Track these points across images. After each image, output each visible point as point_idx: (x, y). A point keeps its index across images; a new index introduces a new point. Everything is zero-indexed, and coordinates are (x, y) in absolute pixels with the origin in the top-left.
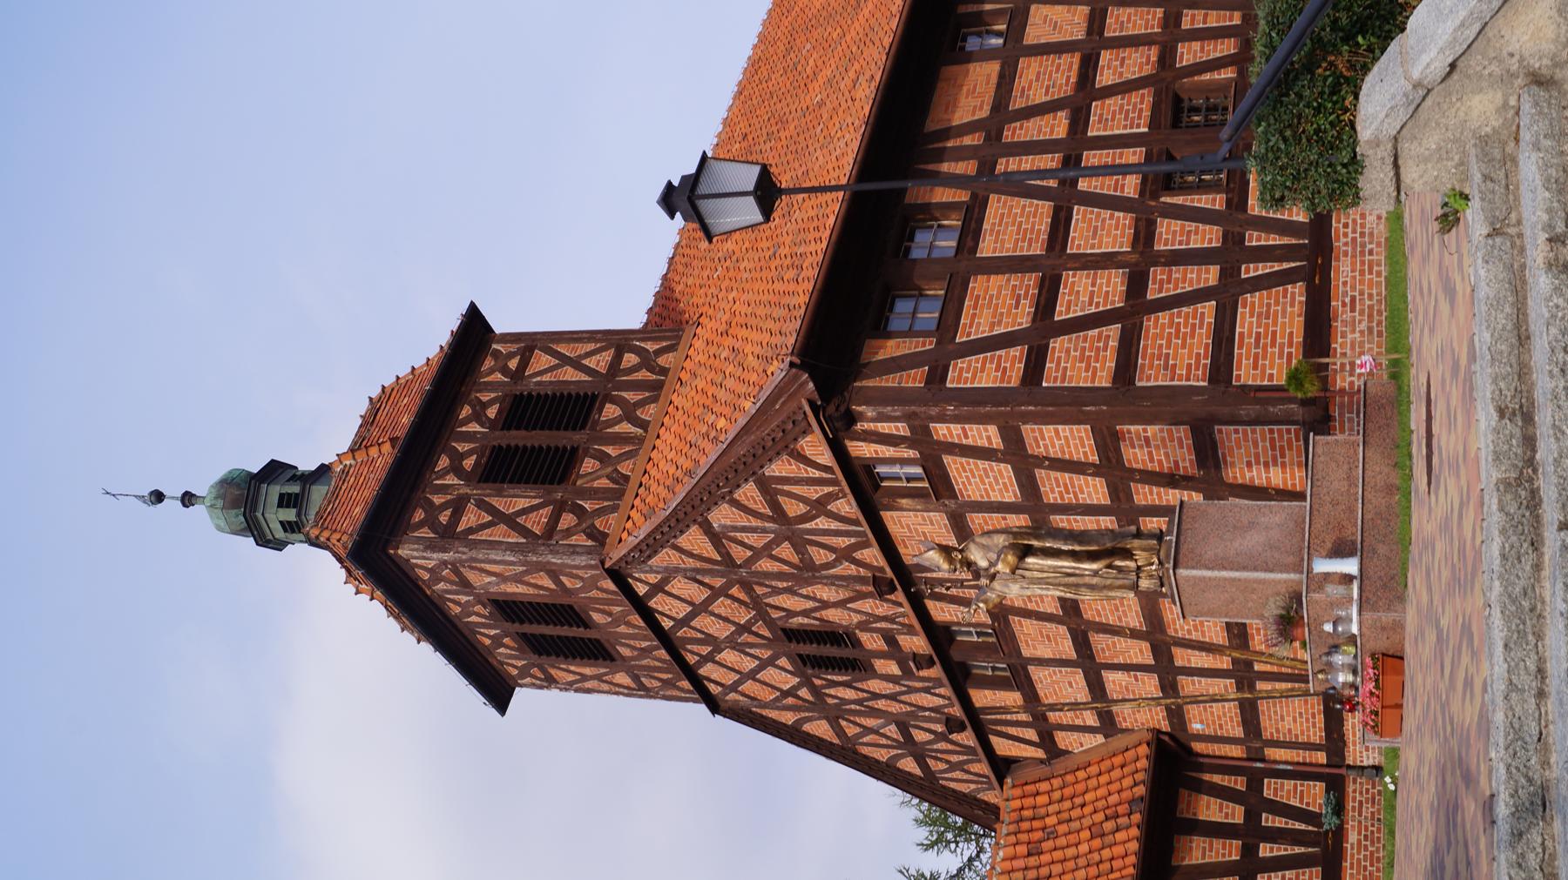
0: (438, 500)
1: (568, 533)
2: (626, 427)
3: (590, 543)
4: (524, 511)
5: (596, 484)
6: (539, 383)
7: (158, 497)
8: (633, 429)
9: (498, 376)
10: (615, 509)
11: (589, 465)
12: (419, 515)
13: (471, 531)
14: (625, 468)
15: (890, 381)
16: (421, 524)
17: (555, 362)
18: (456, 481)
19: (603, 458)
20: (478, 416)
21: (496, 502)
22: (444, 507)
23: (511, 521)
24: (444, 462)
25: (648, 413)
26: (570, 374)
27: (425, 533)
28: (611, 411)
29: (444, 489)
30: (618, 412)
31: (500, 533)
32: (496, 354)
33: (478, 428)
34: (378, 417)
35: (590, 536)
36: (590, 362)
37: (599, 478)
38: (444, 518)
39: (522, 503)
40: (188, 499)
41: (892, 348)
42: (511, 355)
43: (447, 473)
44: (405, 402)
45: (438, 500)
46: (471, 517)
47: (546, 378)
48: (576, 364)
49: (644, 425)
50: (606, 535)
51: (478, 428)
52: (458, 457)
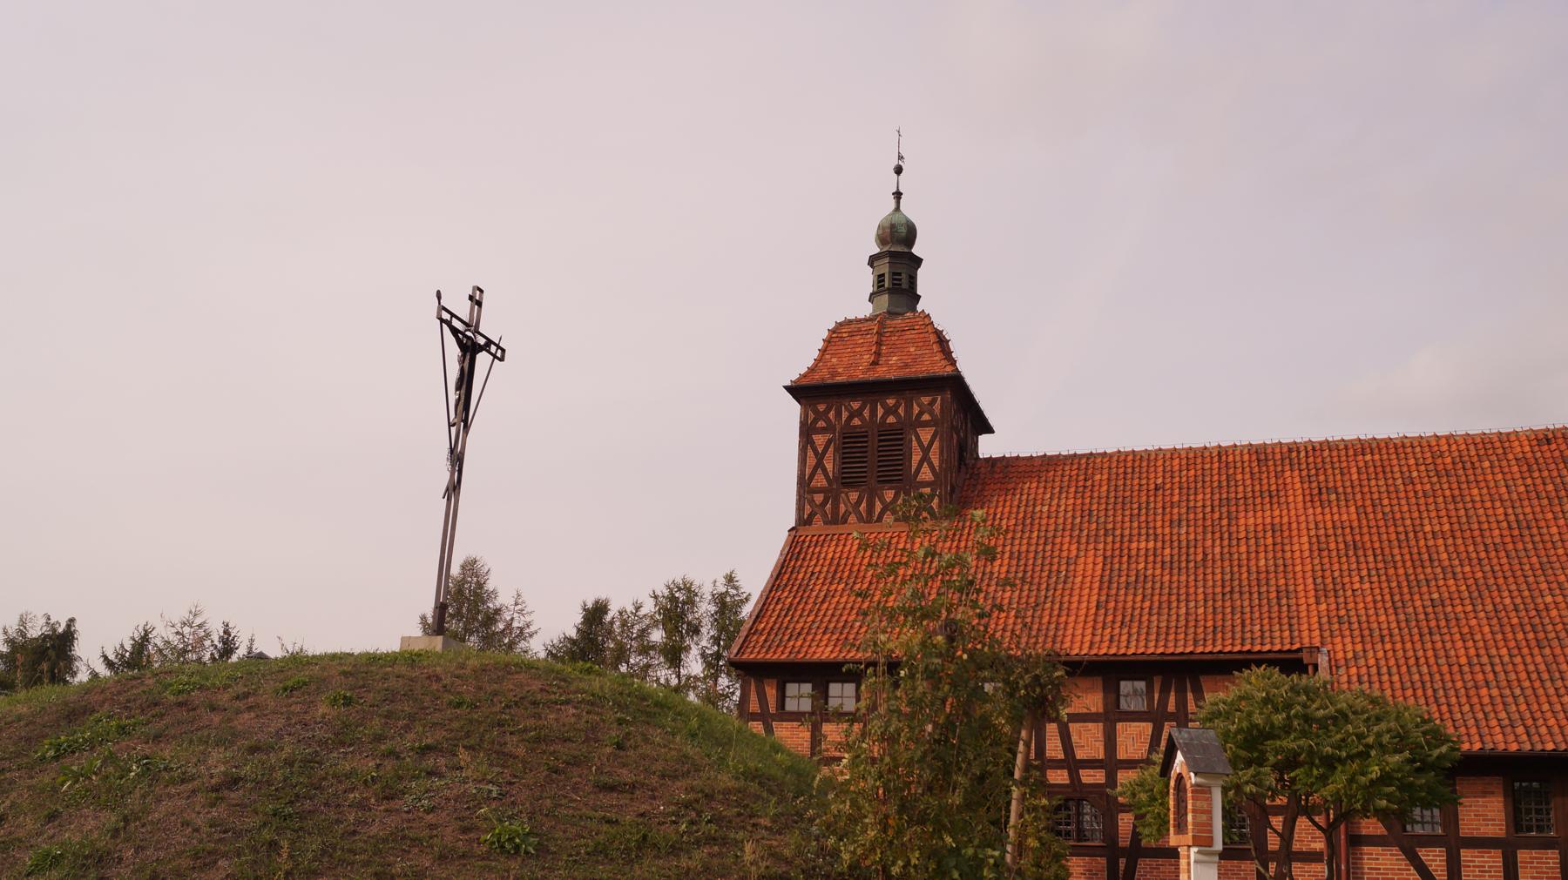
0: (832, 415)
1: (812, 502)
2: (878, 506)
3: (806, 517)
4: (825, 471)
5: (842, 505)
6: (911, 441)
7: (899, 170)
8: (877, 513)
9: (916, 410)
10: (825, 523)
11: (854, 496)
12: (821, 408)
13: (812, 443)
14: (852, 518)
15: (753, 697)
16: (816, 412)
17: (926, 444)
18: (844, 419)
19: (859, 503)
20: (889, 411)
21: (831, 449)
22: (828, 421)
23: (819, 464)
24: (856, 405)
25: (888, 519)
26: (916, 458)
27: (811, 416)
28: (889, 495)
29: (839, 414)
30: (888, 500)
31: (811, 460)
32: (932, 403)
33: (879, 416)
34: (908, 333)
35: (809, 515)
36: (925, 468)
37: (846, 505)
38: (821, 424)
39: (829, 467)
40: (898, 195)
41: (771, 693)
42: (931, 413)
43: (849, 411)
44: (912, 349)
45: (832, 415)
46: (820, 440)
47: (915, 443)
48: (925, 458)
49: (880, 519)
50: (810, 524)
51: (879, 416)
52: (859, 413)
